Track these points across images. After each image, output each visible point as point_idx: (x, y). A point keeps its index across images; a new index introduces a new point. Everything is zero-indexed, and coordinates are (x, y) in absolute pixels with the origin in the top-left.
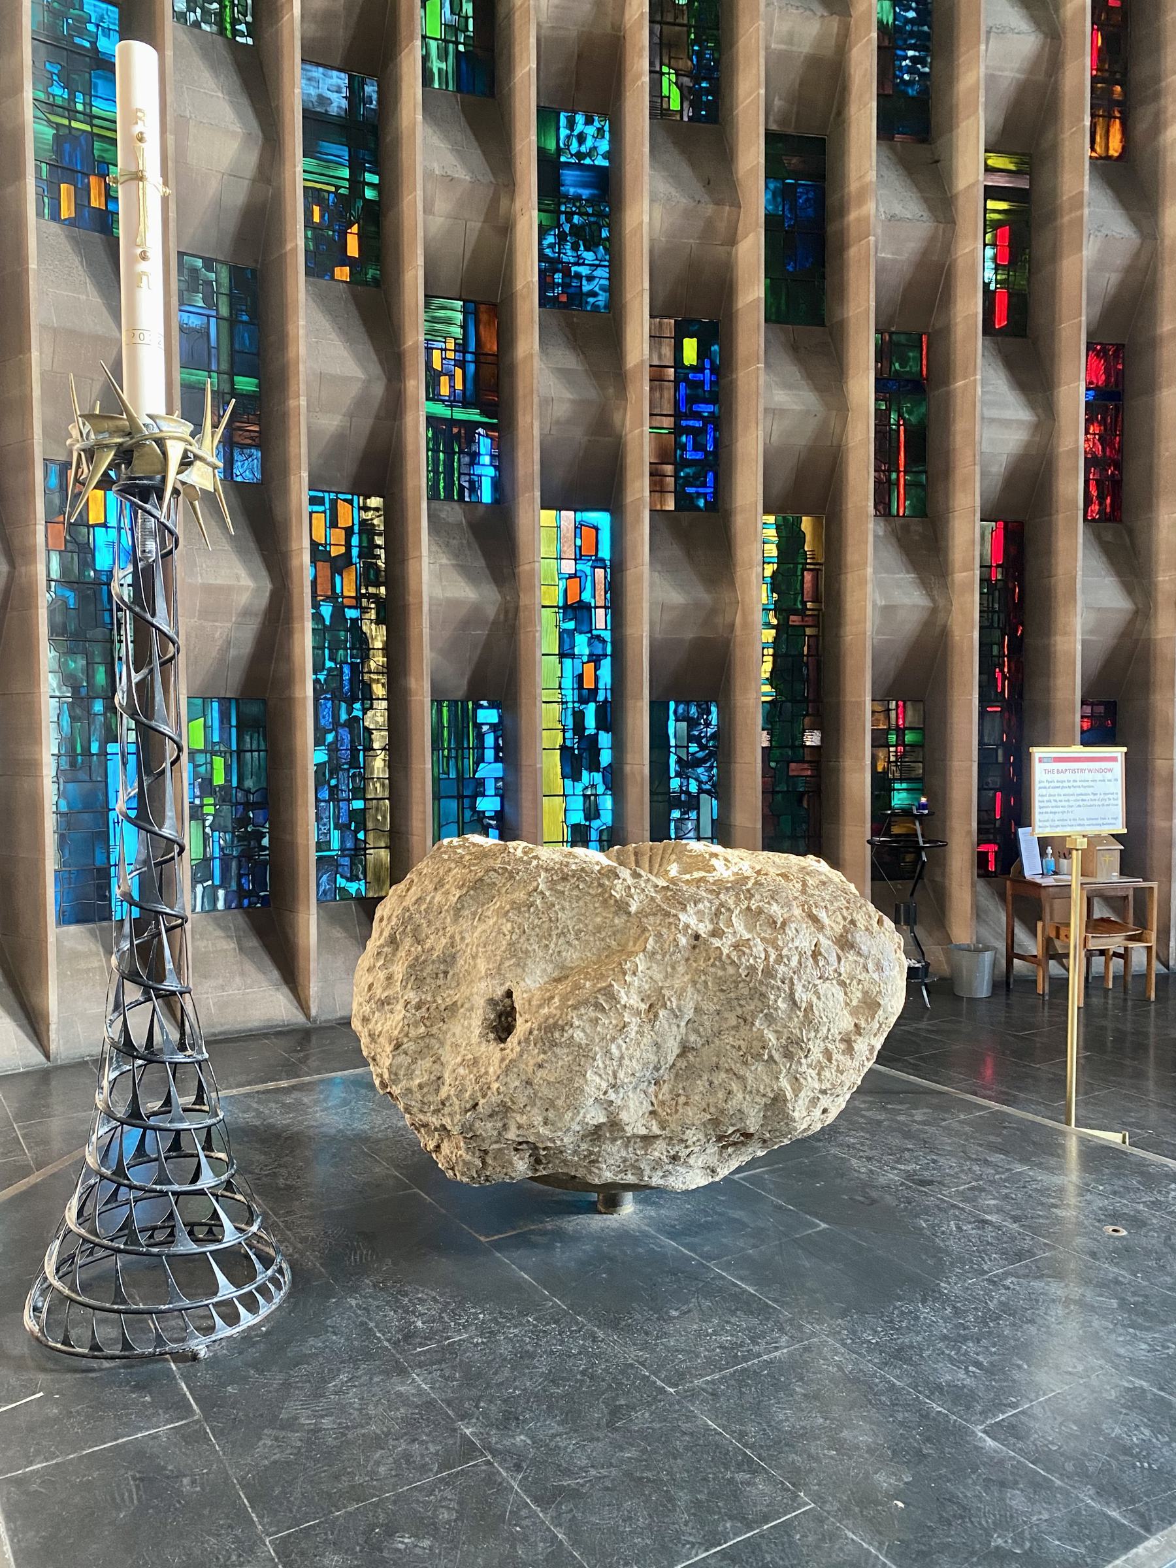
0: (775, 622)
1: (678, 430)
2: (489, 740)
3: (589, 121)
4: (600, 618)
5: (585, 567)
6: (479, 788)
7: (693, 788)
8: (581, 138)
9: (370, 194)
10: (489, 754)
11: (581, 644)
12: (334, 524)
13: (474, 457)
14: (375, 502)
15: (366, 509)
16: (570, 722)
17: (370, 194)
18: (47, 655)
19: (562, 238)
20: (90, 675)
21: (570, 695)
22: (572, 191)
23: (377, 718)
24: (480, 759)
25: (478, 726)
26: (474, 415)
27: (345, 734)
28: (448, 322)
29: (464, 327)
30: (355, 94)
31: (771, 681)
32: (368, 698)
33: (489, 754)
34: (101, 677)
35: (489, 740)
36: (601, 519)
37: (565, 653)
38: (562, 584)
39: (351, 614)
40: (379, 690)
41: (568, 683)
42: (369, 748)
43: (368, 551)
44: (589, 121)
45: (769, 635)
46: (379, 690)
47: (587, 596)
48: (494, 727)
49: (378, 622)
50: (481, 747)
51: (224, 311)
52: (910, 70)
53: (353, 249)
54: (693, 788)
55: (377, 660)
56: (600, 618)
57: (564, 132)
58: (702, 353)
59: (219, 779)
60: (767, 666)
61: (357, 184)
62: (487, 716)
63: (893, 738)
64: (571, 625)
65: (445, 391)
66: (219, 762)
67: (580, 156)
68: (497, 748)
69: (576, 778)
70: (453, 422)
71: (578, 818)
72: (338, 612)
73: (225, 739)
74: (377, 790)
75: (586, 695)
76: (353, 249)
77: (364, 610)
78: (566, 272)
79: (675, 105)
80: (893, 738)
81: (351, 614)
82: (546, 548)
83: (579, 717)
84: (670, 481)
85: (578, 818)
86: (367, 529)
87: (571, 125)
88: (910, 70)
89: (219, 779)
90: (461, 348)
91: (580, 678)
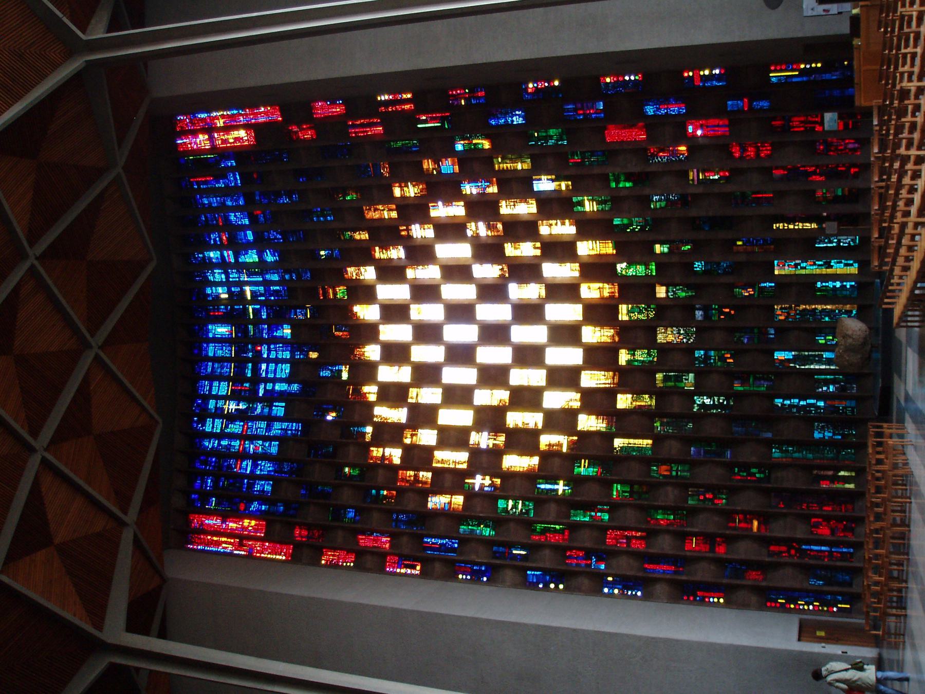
0: (797, 224)
1: (756, 245)
2: (824, 284)
3: (695, 264)
4: (798, 262)
5: (787, 264)
6: (834, 287)
7: (836, 240)
8: (699, 265)
9: (717, 307)
10: (827, 284)
11: (804, 265)
12: (781, 315)
13: (765, 287)
14: (776, 307)
15: (777, 309)
16: (820, 267)
17: (717, 307)
18: (807, 367)
19: (719, 269)
20: (811, 360)
21: (815, 267)
22: (709, 267)
23: (819, 307)
24: (828, 286)
25: (821, 287)
26: (757, 287)
27: (823, 313)
28: (739, 292)
29: (739, 289)
30: (699, 309)
31: (811, 223)
32: (816, 309)
33: (827, 284)
34: (811, 358)
35: (824, 284)
36: (776, 262)
37: (805, 268)
38: (790, 269)
39: (798, 312)
40: (813, 307)
41: (812, 267)
42: (826, 309)
43: (785, 308)
44: (695, 264)
45: (801, 224)
46: (813, 307)
47: (792, 264)
48: (821, 283)
49: (799, 306)
50: (826, 286)
51: (742, 334)
52: (674, 197)
53: (727, 310)
54: (836, 240)
55: (808, 307)
56: (798, 262)
57: (698, 269)
58: (740, 241)
59: (831, 338)
60: (808, 224)
61: (715, 309)
62: (819, 285)
63: (824, 195)
64: (799, 267)
65: (753, 293)
66: (828, 338)
67: (702, 266)
68: (826, 282)
69: (832, 266)
70: (759, 292)
71: (842, 265)
72: (798, 314)
73: (823, 336)
74: (834, 307)
75: (815, 264)
76: (727, 310)
77: (797, 309)
78: (725, 269)
79: (689, 247)
80: (824, 195)
81: (798, 312)
82: (783, 273)
83: (819, 265)
84: (768, 247)
85: (842, 265)
86: (781, 308)
87: (696, 268)
88: (674, 197)
89: (831, 338)
90: (743, 289)
91: (811, 265)
